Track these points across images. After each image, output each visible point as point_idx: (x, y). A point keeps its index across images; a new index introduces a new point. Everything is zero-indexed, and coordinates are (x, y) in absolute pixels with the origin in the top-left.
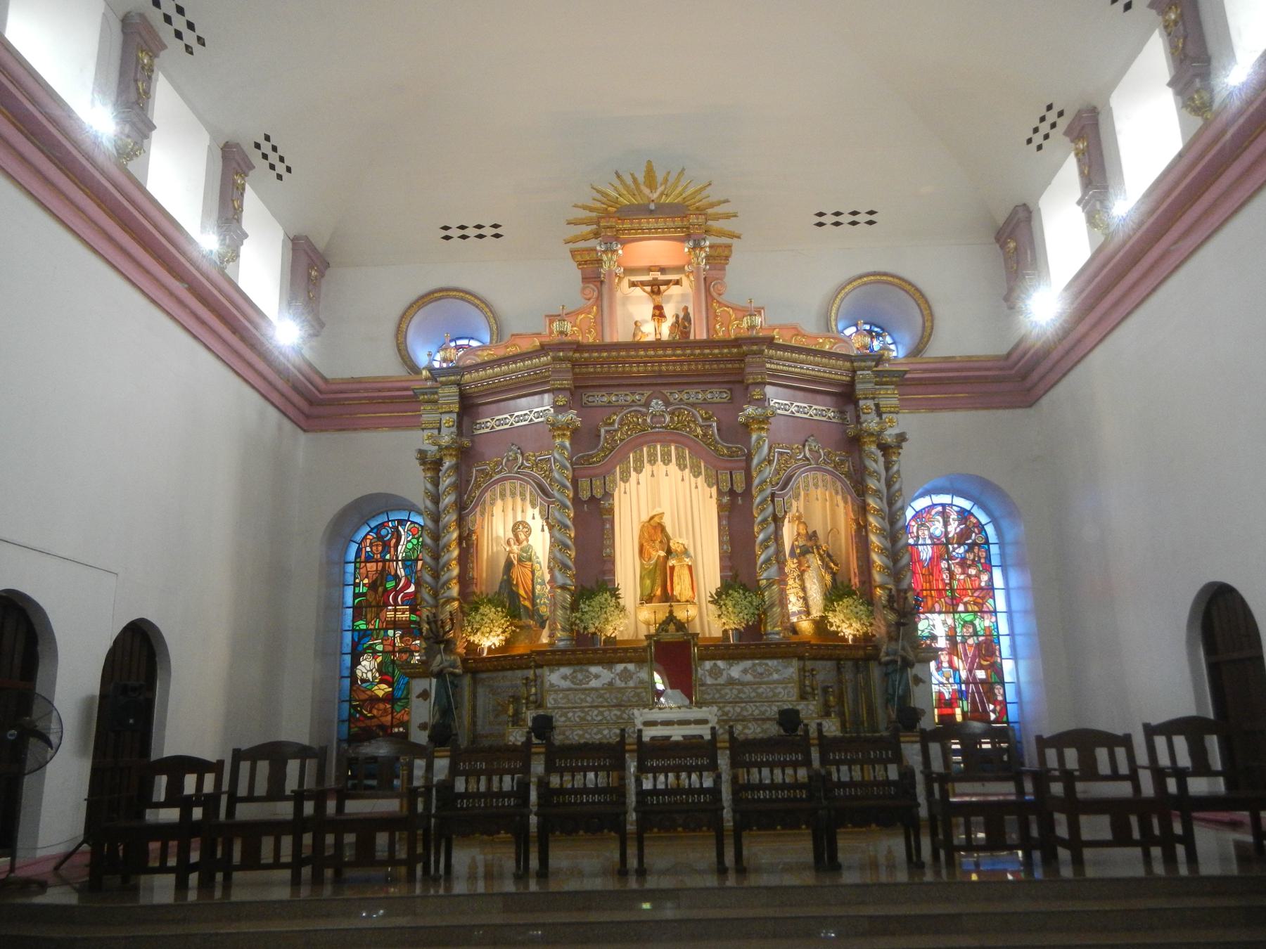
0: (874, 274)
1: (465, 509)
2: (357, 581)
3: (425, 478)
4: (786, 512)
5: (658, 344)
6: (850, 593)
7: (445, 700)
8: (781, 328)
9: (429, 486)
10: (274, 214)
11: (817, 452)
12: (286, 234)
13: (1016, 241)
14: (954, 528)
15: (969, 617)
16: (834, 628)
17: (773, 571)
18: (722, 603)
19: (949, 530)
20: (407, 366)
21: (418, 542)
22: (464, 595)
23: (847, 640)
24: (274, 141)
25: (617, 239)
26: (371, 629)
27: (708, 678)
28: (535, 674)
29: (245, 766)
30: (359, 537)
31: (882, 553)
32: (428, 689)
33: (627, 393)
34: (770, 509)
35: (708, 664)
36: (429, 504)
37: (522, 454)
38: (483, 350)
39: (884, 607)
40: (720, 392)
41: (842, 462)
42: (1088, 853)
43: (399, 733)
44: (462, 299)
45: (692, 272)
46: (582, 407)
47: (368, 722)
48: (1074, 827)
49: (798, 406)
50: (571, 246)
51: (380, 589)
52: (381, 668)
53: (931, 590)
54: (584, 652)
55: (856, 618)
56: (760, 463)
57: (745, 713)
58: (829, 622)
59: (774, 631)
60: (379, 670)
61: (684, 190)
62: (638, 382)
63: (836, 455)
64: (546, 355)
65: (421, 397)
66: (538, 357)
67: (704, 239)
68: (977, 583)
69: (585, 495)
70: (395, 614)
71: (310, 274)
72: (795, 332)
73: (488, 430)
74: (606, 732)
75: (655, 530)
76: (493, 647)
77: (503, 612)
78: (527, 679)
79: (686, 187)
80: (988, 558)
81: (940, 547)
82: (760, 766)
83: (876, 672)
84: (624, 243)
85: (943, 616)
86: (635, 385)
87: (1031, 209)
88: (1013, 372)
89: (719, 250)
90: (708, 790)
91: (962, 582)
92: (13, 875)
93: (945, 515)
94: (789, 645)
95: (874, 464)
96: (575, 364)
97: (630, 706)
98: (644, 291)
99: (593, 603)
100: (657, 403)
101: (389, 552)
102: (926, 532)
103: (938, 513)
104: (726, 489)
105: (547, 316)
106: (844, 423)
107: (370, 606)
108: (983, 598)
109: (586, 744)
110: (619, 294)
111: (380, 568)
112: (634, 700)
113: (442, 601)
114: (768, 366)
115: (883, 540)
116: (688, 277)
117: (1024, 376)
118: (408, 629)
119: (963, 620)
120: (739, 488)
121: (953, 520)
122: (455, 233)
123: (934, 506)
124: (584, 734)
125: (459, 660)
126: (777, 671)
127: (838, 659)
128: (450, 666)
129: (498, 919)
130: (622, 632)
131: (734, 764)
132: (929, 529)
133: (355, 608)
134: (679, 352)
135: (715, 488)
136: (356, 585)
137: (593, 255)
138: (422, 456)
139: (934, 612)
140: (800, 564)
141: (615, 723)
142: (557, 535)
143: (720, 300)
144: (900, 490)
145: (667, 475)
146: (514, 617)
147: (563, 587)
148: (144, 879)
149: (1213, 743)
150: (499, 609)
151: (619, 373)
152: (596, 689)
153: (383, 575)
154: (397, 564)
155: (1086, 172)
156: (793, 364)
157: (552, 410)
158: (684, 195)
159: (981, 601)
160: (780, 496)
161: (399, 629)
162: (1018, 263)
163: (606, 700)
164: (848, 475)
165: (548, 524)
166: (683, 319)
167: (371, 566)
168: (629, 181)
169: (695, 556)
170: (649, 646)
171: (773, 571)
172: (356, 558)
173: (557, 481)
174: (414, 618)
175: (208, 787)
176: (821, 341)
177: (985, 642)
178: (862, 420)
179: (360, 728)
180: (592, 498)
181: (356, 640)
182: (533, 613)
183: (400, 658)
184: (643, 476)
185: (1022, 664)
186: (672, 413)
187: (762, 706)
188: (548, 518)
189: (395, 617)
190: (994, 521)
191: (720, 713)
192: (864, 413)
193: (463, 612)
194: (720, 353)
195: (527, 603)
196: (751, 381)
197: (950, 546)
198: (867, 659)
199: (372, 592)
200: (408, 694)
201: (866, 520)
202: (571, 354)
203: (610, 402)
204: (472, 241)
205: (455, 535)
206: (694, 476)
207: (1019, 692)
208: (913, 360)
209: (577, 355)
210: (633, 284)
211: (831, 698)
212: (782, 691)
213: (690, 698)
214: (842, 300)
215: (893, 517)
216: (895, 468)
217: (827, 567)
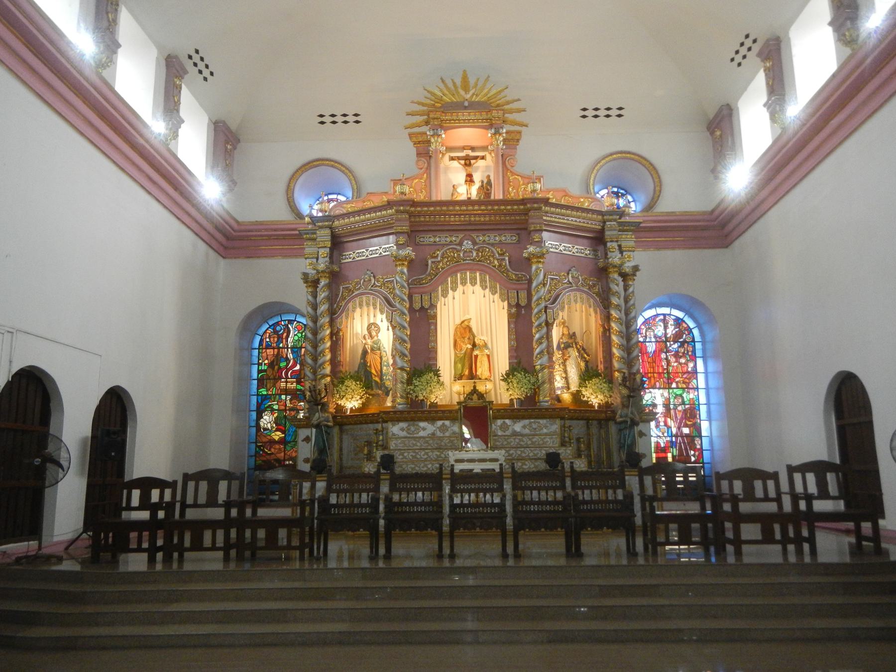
0: (621, 152)
1: (335, 314)
2: (260, 361)
3: (307, 292)
4: (554, 319)
5: (469, 202)
6: (597, 375)
7: (321, 443)
8: (556, 190)
9: (310, 298)
10: (201, 105)
11: (577, 278)
12: (210, 119)
13: (721, 130)
14: (671, 331)
15: (679, 392)
16: (585, 399)
17: (545, 358)
18: (510, 381)
19: (667, 332)
20: (295, 213)
21: (302, 335)
22: (334, 373)
23: (594, 407)
24: (201, 54)
25: (442, 127)
26: (270, 395)
27: (499, 431)
28: (382, 427)
29: (191, 485)
30: (261, 332)
31: (620, 348)
32: (310, 436)
33: (448, 235)
34: (544, 317)
35: (499, 422)
36: (310, 309)
37: (374, 277)
38: (347, 204)
39: (620, 384)
40: (511, 236)
41: (594, 285)
42: (745, 548)
43: (289, 464)
44: (332, 166)
45: (493, 150)
46: (416, 245)
47: (268, 457)
48: (737, 531)
49: (565, 246)
50: (409, 130)
51: (276, 367)
53: (654, 373)
54: (415, 412)
55: (601, 392)
56: (537, 286)
57: (524, 455)
58: (582, 394)
59: (545, 400)
60: (276, 423)
61: (489, 92)
62: (455, 228)
63: (590, 280)
64: (391, 209)
65: (305, 236)
66: (386, 210)
67: (502, 128)
68: (685, 369)
69: (417, 306)
70: (286, 385)
71: (226, 148)
72: (564, 194)
73: (350, 260)
74: (430, 466)
75: (465, 331)
76: (354, 408)
77: (360, 384)
78: (377, 430)
79: (490, 90)
80: (694, 351)
81: (661, 343)
82: (531, 489)
83: (613, 428)
85: (661, 391)
86: (453, 230)
87: (733, 107)
88: (716, 223)
89: (513, 135)
90: (497, 505)
91: (675, 368)
92: (40, 552)
93: (665, 322)
94: (554, 409)
95: (616, 287)
96: (411, 215)
97: (446, 449)
98: (460, 163)
99: (422, 380)
100: (467, 243)
101: (282, 342)
102: (652, 333)
103: (660, 320)
104: (514, 303)
105: (391, 180)
106: (596, 258)
107: (270, 379)
108: (689, 379)
109: (417, 474)
110: (442, 165)
111: (276, 353)
112: (449, 445)
113: (319, 377)
114: (545, 218)
115: (621, 339)
116: (490, 154)
117: (723, 225)
118: (296, 395)
119: (675, 394)
120: (523, 302)
121: (671, 325)
122: (328, 119)
123: (657, 315)
124: (415, 468)
125: (331, 417)
126: (546, 427)
127: (587, 420)
128: (325, 421)
129: (360, 585)
130: (441, 400)
131: (515, 487)
132: (654, 331)
133: (258, 379)
134: (483, 208)
135: (506, 302)
136: (259, 364)
137: (424, 138)
138: (305, 276)
139: (656, 388)
140: (563, 354)
141: (436, 460)
142: (398, 333)
143: (512, 170)
144: (634, 304)
145: (473, 293)
146: (367, 388)
147: (402, 369)
148: (122, 557)
149: (830, 477)
150: (358, 383)
151: (442, 222)
152: (423, 437)
153: (278, 358)
154: (288, 350)
155: (770, 83)
156: (562, 217)
157: (395, 247)
158: (488, 96)
159: (688, 381)
160: (550, 308)
161: (289, 395)
162: (721, 146)
163: (430, 445)
164: (598, 294)
165: (392, 325)
166: (487, 183)
167: (270, 352)
168: (450, 85)
169: (492, 348)
170: (460, 409)
171: (545, 358)
172: (259, 346)
173: (398, 296)
174: (299, 387)
175: (168, 497)
176: (582, 200)
177: (690, 408)
178: (609, 257)
179: (264, 461)
180: (422, 308)
181: (260, 401)
182: (381, 385)
183: (290, 414)
184: (457, 294)
185: (714, 424)
186: (478, 250)
187: (536, 450)
188: (392, 321)
189: (286, 386)
190: (699, 326)
191: (507, 454)
192: (610, 252)
193: (333, 384)
194: (511, 209)
195: (377, 379)
196: (532, 229)
197: (668, 344)
198: (608, 420)
199: (271, 370)
200: (295, 438)
201: (609, 325)
202: (408, 208)
203: (435, 242)
204: (340, 124)
205: (328, 332)
206: (492, 294)
207: (711, 443)
208: (646, 214)
209: (413, 209)
210: (452, 159)
211: (582, 445)
212: (549, 440)
213: (486, 443)
214: (598, 171)
215: (628, 323)
216: (631, 290)
217: (582, 357)
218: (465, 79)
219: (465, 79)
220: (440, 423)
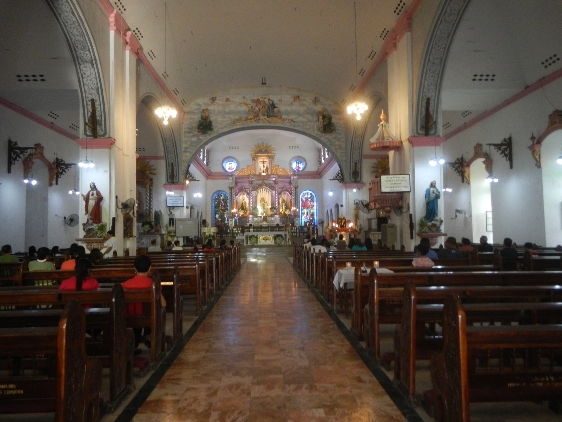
14: (309, 196)
15: (310, 210)
52: (220, 216)
75: (263, 199)
84: (259, 157)
138: (229, 187)
167: (217, 200)
218: (263, 143)
219: (263, 143)
220: (258, 218)
